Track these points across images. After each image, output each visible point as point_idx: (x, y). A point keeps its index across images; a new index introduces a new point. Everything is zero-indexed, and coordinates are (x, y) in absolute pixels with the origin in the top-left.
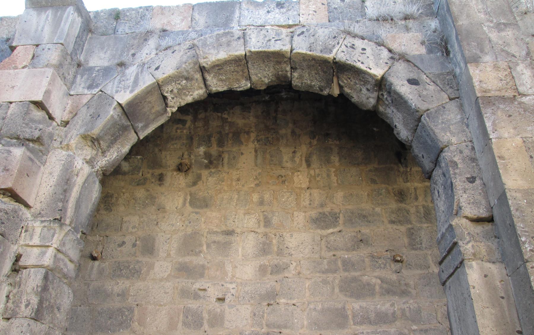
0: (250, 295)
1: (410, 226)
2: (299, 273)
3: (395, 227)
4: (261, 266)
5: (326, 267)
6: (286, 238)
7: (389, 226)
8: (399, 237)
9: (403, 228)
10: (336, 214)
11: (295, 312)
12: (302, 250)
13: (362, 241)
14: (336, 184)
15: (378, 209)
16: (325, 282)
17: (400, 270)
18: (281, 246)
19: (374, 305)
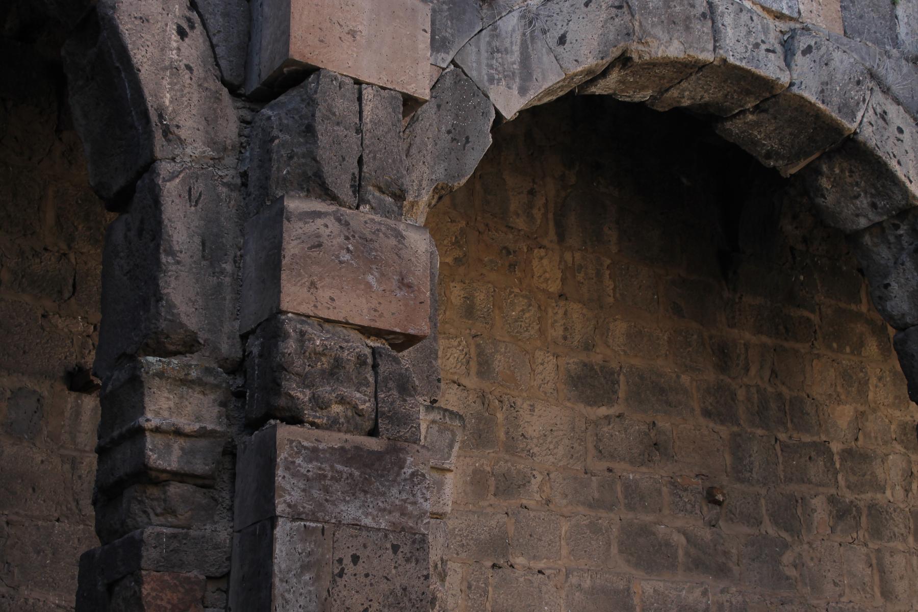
0: (458, 538)
1: (735, 429)
2: (548, 502)
3: (711, 425)
4: (475, 472)
5: (596, 495)
6: (521, 412)
7: (702, 421)
8: (718, 450)
9: (724, 431)
10: (612, 373)
11: (544, 589)
12: (552, 447)
13: (655, 447)
14: (611, 300)
15: (685, 379)
16: (594, 528)
17: (717, 521)
18: (512, 430)
19: (676, 589)
